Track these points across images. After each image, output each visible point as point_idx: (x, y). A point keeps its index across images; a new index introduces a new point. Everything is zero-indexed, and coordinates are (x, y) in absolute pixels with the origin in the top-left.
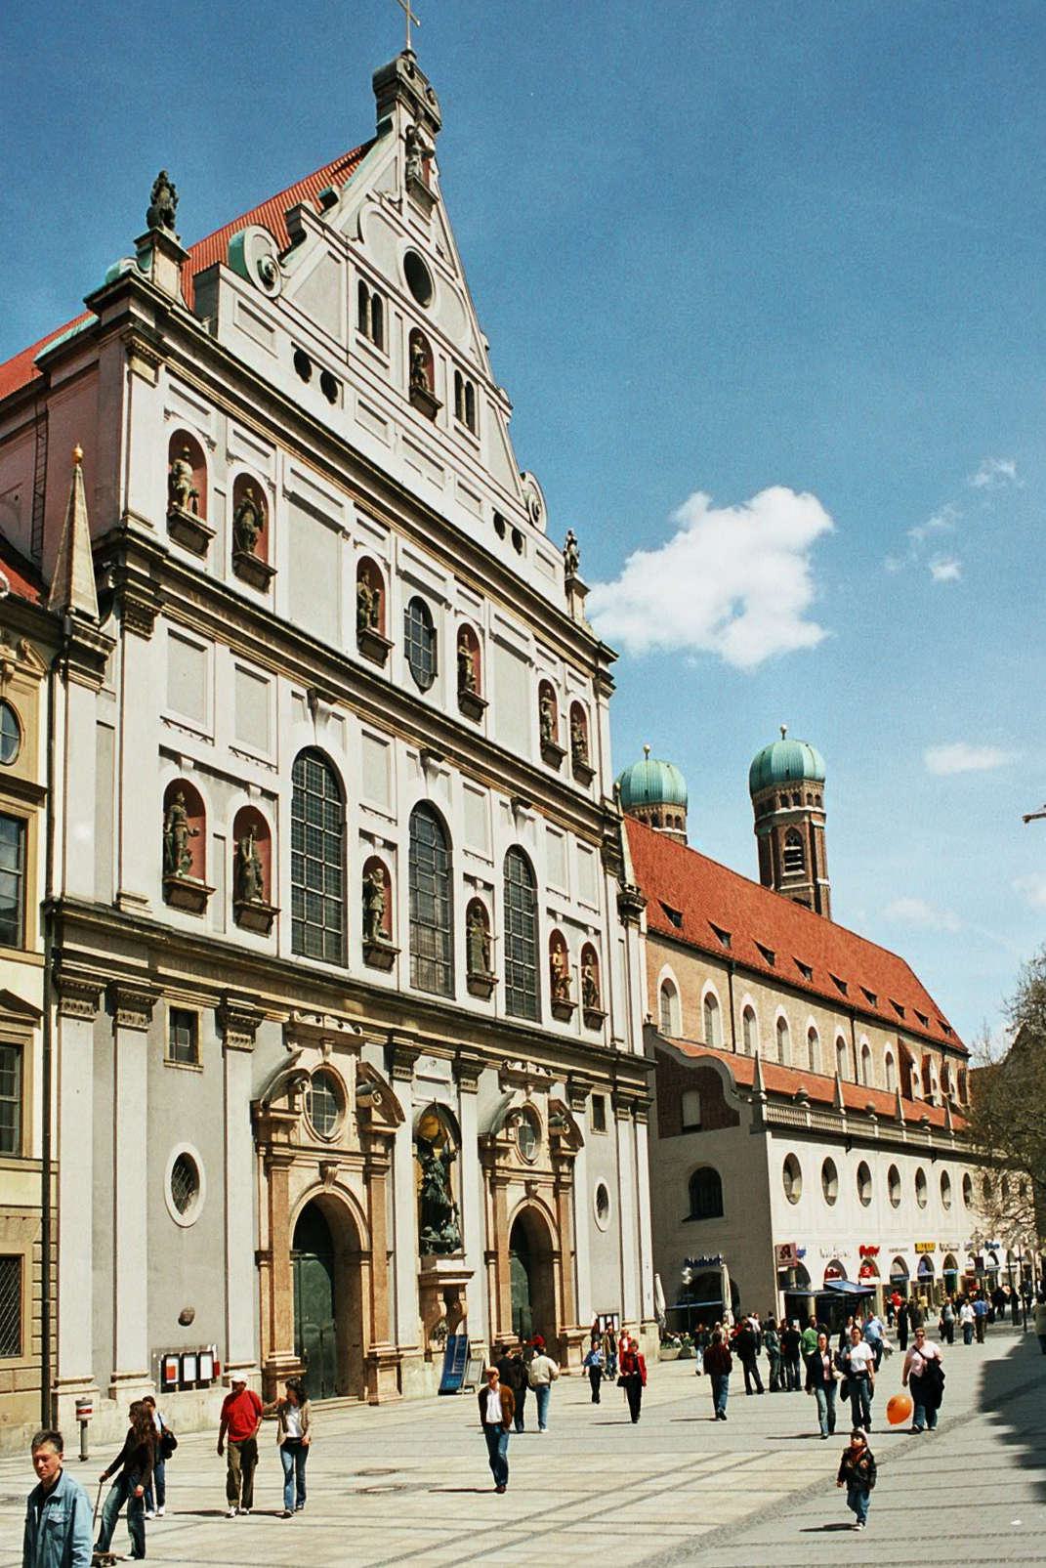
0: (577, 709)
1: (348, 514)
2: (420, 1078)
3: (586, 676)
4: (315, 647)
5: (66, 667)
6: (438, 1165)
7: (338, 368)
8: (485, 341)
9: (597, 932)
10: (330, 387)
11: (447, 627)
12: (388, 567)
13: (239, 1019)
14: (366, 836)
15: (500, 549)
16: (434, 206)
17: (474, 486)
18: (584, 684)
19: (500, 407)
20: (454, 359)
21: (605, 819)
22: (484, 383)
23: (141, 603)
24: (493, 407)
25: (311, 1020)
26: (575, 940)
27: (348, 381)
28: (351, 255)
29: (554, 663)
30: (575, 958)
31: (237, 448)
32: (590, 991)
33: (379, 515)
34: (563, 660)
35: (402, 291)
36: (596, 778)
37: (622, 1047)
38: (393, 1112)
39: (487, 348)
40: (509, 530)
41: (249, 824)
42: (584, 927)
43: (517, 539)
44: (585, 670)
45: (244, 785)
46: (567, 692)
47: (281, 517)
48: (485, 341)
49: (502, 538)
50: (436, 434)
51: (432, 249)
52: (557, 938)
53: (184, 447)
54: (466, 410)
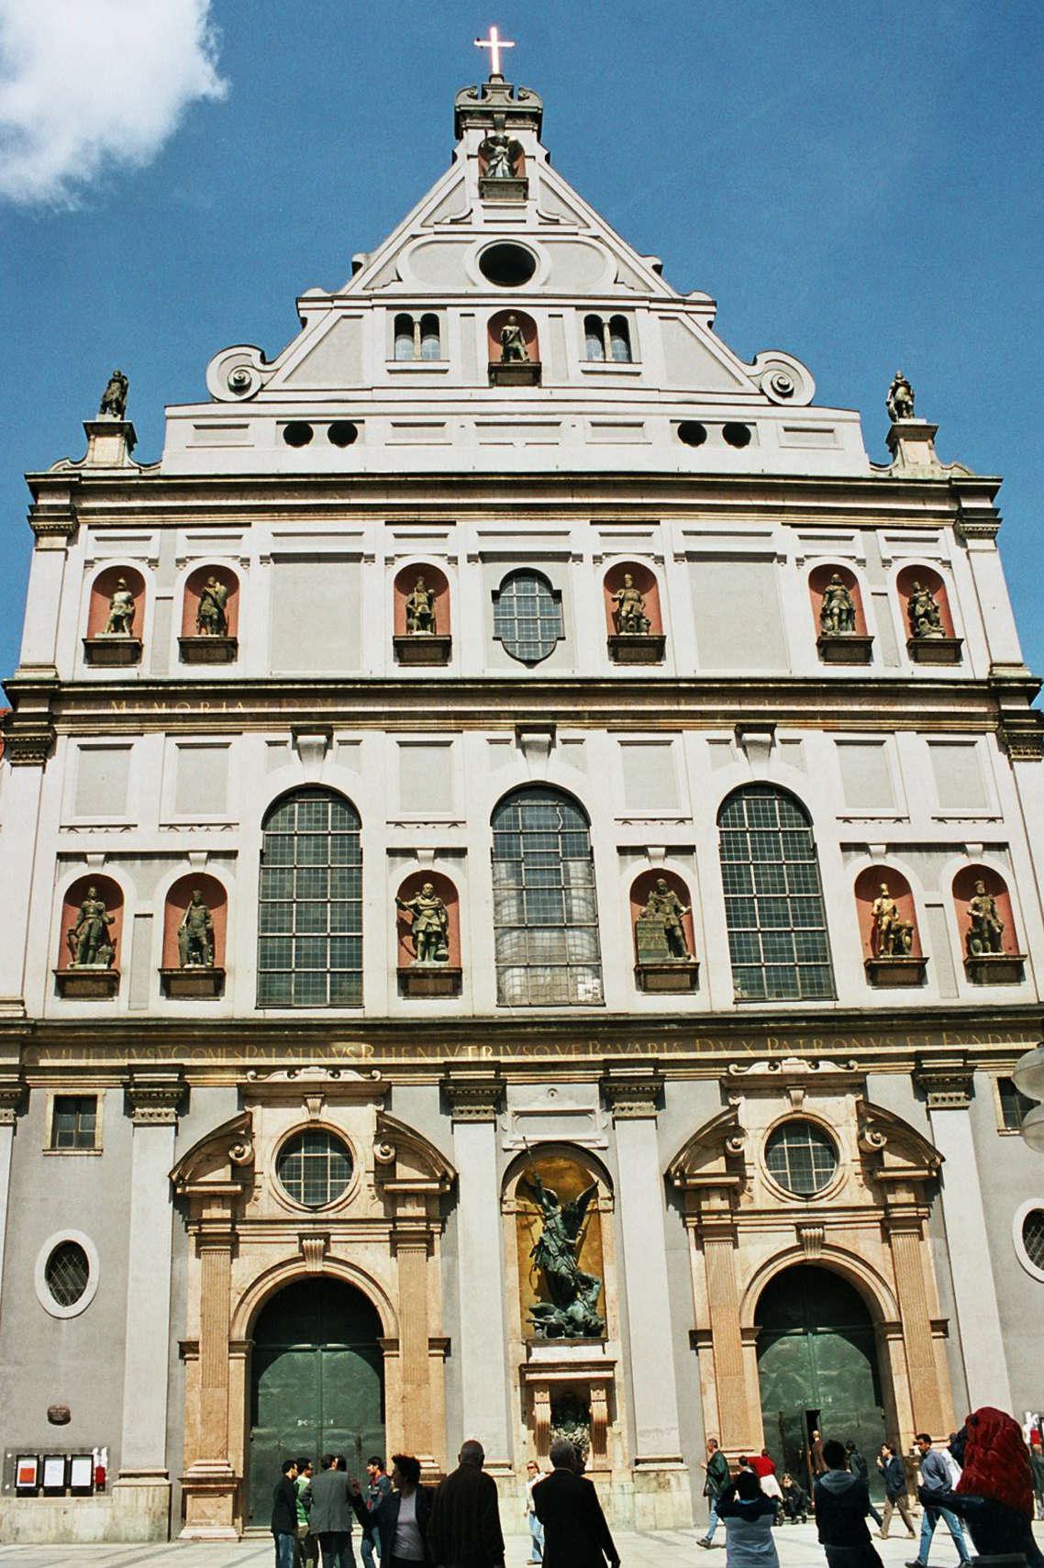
4: (297, 686)
7: (340, 412)
10: (343, 433)
13: (144, 1093)
17: (627, 414)
19: (687, 312)
20: (578, 308)
22: (646, 303)
23: (24, 738)
24: (676, 318)
25: (280, 1077)
27: (364, 415)
28: (375, 302)
33: (434, 516)
39: (658, 269)
43: (737, 435)
51: (533, 224)
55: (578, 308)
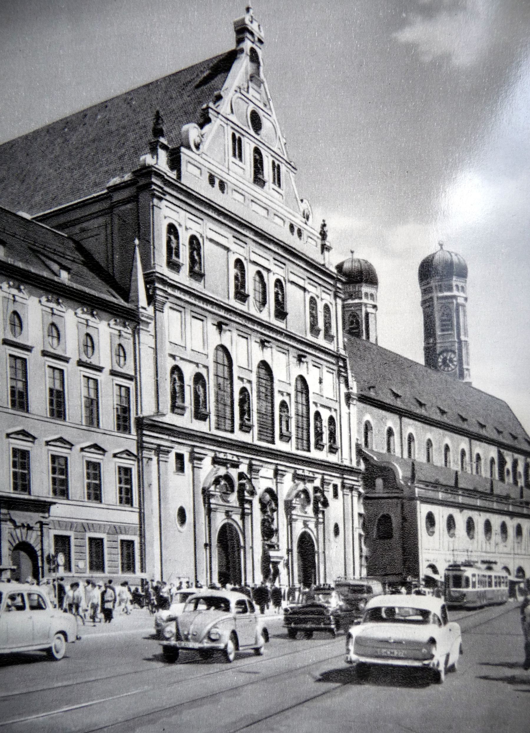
0: (327, 308)
1: (230, 242)
2: (261, 477)
3: (330, 290)
5: (139, 329)
6: (269, 513)
7: (226, 177)
8: (285, 141)
9: (335, 410)
10: (222, 186)
11: (270, 281)
12: (246, 259)
14: (241, 379)
15: (292, 241)
16: (262, 85)
18: (330, 295)
21: (338, 357)
26: (325, 415)
29: (316, 287)
30: (325, 423)
31: (190, 224)
32: (332, 436)
34: (320, 285)
35: (249, 131)
36: (335, 339)
37: (347, 463)
38: (252, 493)
40: (296, 229)
41: (199, 378)
42: (329, 408)
44: (330, 287)
45: (197, 364)
46: (322, 299)
47: (207, 248)
48: (285, 141)
49: (293, 234)
50: (265, 194)
52: (318, 415)
53: (172, 229)
54: (277, 180)
55: (272, 156)
